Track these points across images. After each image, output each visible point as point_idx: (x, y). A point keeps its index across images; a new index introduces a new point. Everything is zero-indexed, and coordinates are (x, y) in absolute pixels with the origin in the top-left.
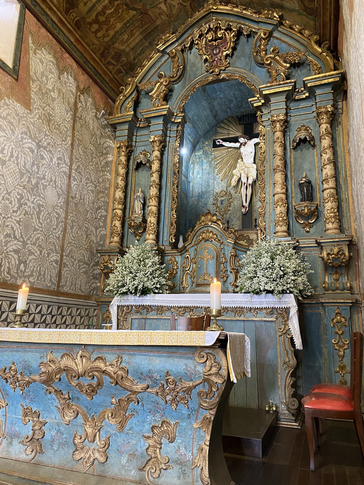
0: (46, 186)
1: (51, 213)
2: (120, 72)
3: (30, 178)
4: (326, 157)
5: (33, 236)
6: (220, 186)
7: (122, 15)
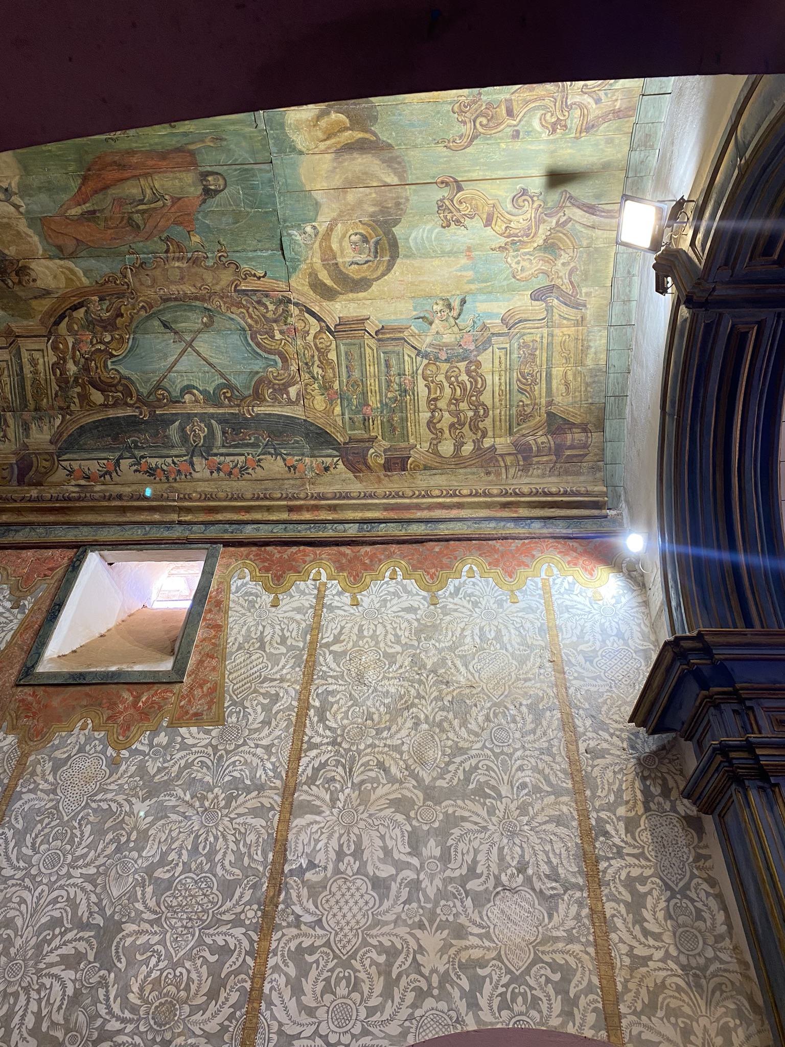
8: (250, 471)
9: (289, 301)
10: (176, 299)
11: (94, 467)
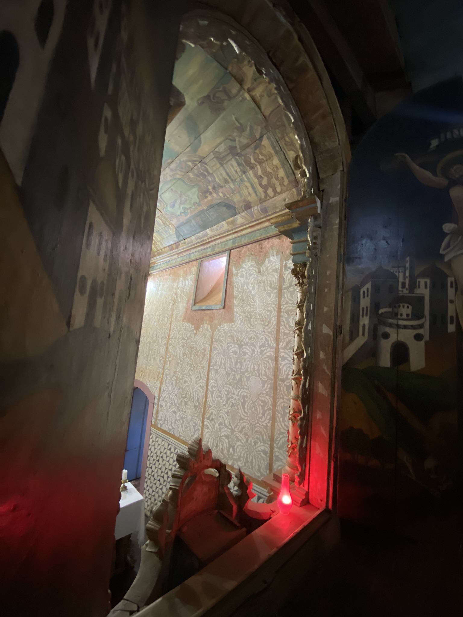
0: (249, 377)
1: (256, 401)
3: (234, 375)
5: (239, 424)
7: (265, 156)
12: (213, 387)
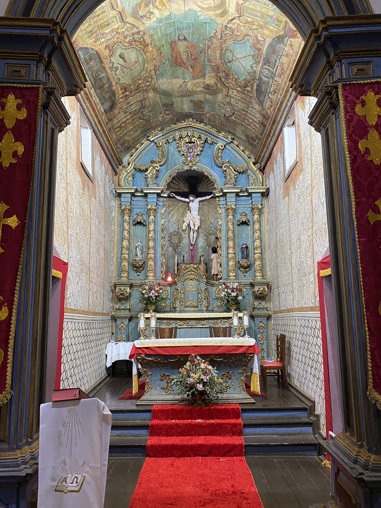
2: (121, 151)
4: (257, 235)
6: (173, 228)
8: (284, 68)
9: (226, 26)
10: (221, 56)
11: (268, 103)
12: (92, 253)
